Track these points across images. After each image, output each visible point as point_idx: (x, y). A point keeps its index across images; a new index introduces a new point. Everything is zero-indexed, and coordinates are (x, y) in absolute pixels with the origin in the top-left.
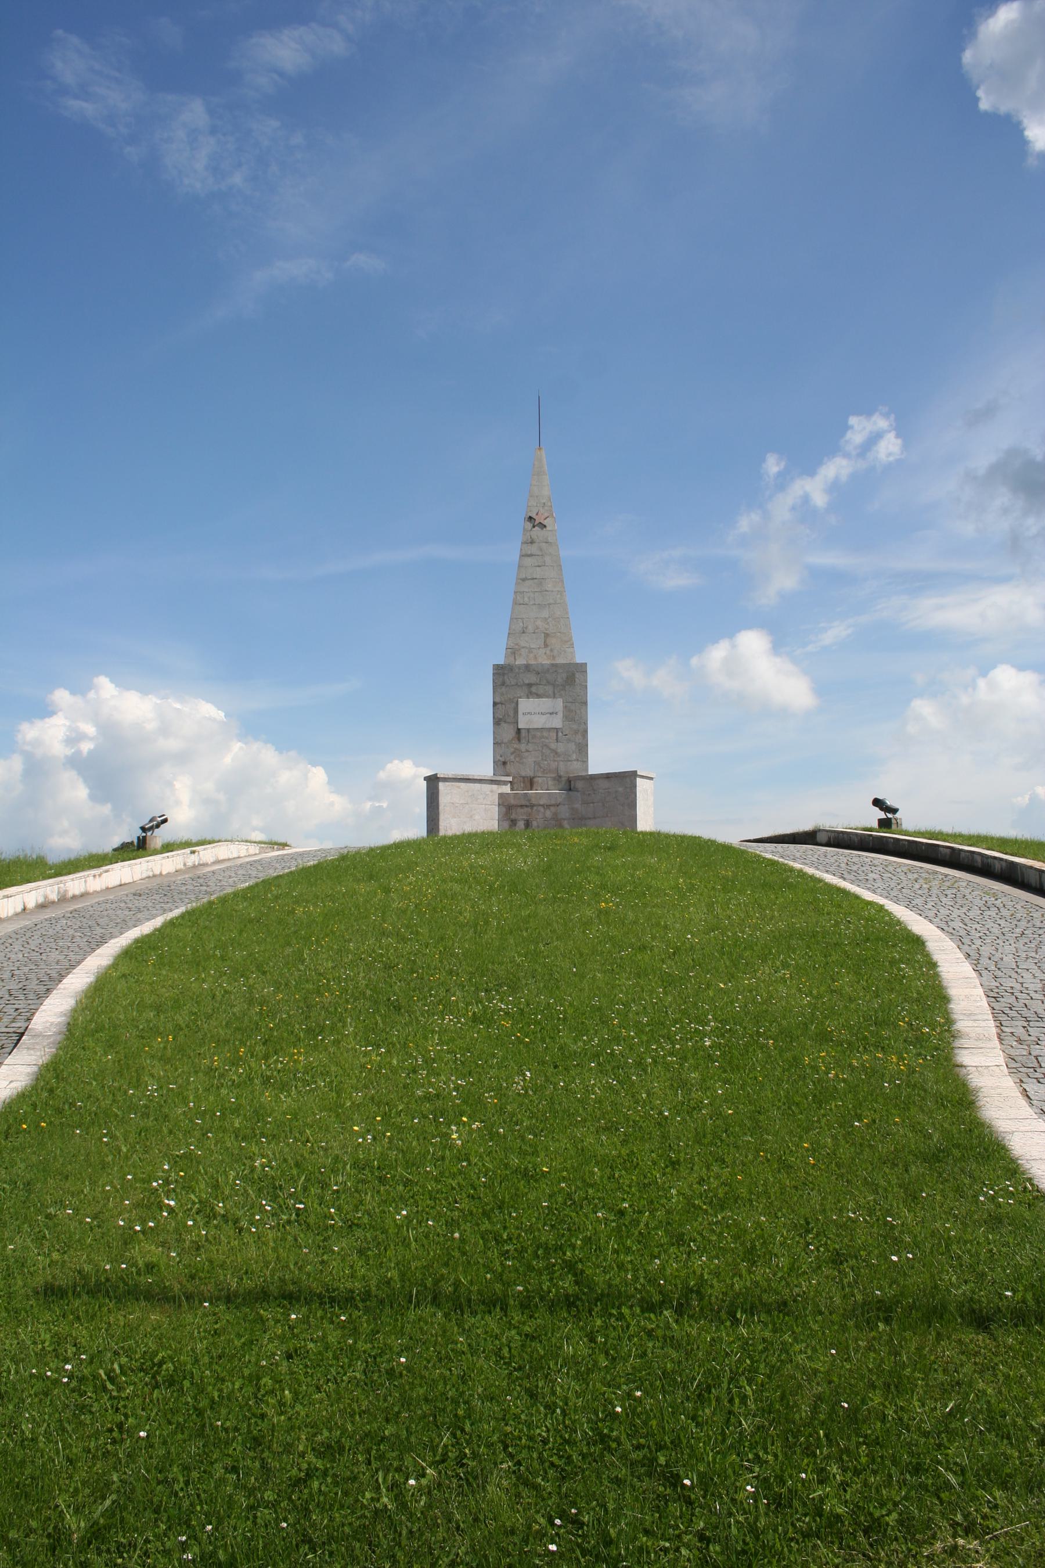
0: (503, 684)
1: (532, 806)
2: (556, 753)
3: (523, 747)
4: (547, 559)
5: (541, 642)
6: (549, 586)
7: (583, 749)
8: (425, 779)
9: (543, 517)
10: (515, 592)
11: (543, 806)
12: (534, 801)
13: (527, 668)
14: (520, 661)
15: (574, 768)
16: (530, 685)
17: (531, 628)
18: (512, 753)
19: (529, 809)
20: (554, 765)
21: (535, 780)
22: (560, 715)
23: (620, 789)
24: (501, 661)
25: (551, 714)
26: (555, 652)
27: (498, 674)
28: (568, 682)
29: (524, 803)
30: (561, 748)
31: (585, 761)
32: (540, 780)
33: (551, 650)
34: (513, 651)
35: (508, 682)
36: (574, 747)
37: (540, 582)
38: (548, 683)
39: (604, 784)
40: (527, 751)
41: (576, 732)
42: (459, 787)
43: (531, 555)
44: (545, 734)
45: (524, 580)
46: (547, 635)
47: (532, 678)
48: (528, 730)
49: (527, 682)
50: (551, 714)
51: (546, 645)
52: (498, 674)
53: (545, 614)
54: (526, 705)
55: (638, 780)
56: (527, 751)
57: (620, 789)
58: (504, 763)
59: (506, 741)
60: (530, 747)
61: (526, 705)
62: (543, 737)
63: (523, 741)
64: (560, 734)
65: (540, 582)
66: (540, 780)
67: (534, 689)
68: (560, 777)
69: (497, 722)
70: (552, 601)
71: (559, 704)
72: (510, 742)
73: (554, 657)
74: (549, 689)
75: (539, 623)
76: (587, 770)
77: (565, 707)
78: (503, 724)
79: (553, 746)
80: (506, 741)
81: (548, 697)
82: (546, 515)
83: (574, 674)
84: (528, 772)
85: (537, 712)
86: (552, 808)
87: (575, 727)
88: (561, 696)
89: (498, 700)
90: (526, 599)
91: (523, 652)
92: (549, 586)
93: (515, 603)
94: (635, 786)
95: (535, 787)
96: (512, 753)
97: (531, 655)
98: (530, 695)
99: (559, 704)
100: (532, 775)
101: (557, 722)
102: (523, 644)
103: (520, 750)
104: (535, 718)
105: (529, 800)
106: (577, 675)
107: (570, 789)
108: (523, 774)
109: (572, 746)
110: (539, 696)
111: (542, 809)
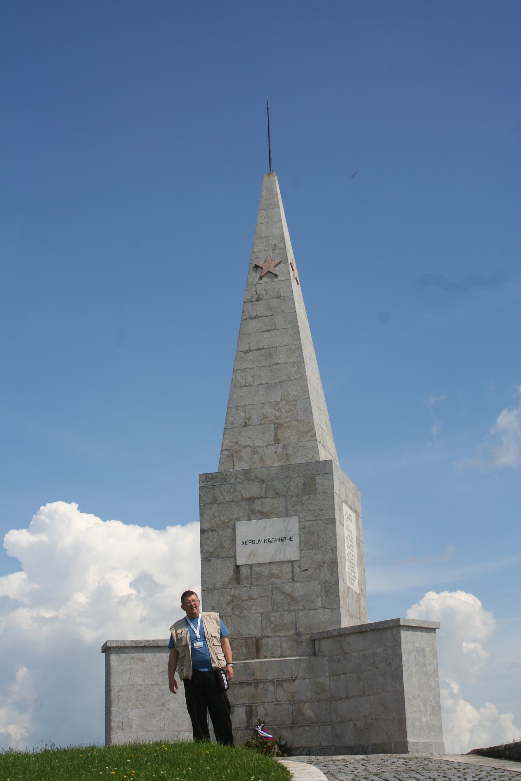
0: (214, 501)
1: (257, 683)
2: (293, 599)
3: (244, 592)
4: (279, 320)
5: (269, 437)
6: (282, 358)
7: (331, 589)
9: (273, 264)
10: (235, 371)
11: (272, 681)
12: (259, 676)
13: (248, 475)
14: (241, 466)
15: (321, 618)
16: (251, 500)
17: (255, 419)
18: (228, 604)
19: (252, 689)
20: (289, 618)
21: (264, 641)
22: (296, 540)
23: (380, 650)
24: (213, 468)
25: (283, 540)
26: (290, 450)
27: (208, 487)
28: (304, 490)
29: (244, 679)
30: (299, 590)
32: (269, 642)
33: (284, 447)
34: (230, 454)
35: (221, 499)
36: (318, 588)
37: (269, 352)
38: (278, 494)
39: (356, 643)
40: (251, 598)
41: (320, 566)
42: (143, 660)
43: (257, 317)
44: (275, 570)
45: (246, 352)
46: (278, 426)
47: (254, 489)
48: (251, 566)
49: (247, 496)
50: (283, 540)
51: (277, 441)
52: (208, 487)
53: (276, 396)
54: (245, 530)
55: (404, 635)
56: (251, 598)
57: (380, 650)
59: (219, 585)
60: (255, 592)
61: (245, 530)
62: (271, 576)
63: (245, 583)
64: (297, 569)
65: (269, 352)
66: (269, 642)
68: (299, 634)
70: (285, 378)
71: (292, 525)
72: (225, 586)
73: (288, 457)
74: (279, 503)
75: (268, 410)
76: (339, 622)
77: (302, 529)
78: (214, 561)
79: (288, 588)
80: (219, 585)
81: (278, 515)
82: (277, 260)
83: (313, 479)
84: (252, 629)
85: (263, 540)
86: (286, 685)
87: (319, 557)
88: (296, 513)
89: (207, 526)
90: (250, 378)
91: (246, 453)
92: (282, 358)
93: (234, 385)
94: (399, 645)
95: (263, 653)
96: (228, 604)
97: (256, 457)
98: (253, 514)
99: (292, 525)
100: (259, 635)
101: (291, 552)
102: (244, 441)
103: (240, 598)
104: (261, 548)
105: (253, 674)
106: (318, 479)
107: (315, 654)
108: (245, 633)
109: (316, 587)
110: (265, 515)
111: (271, 688)
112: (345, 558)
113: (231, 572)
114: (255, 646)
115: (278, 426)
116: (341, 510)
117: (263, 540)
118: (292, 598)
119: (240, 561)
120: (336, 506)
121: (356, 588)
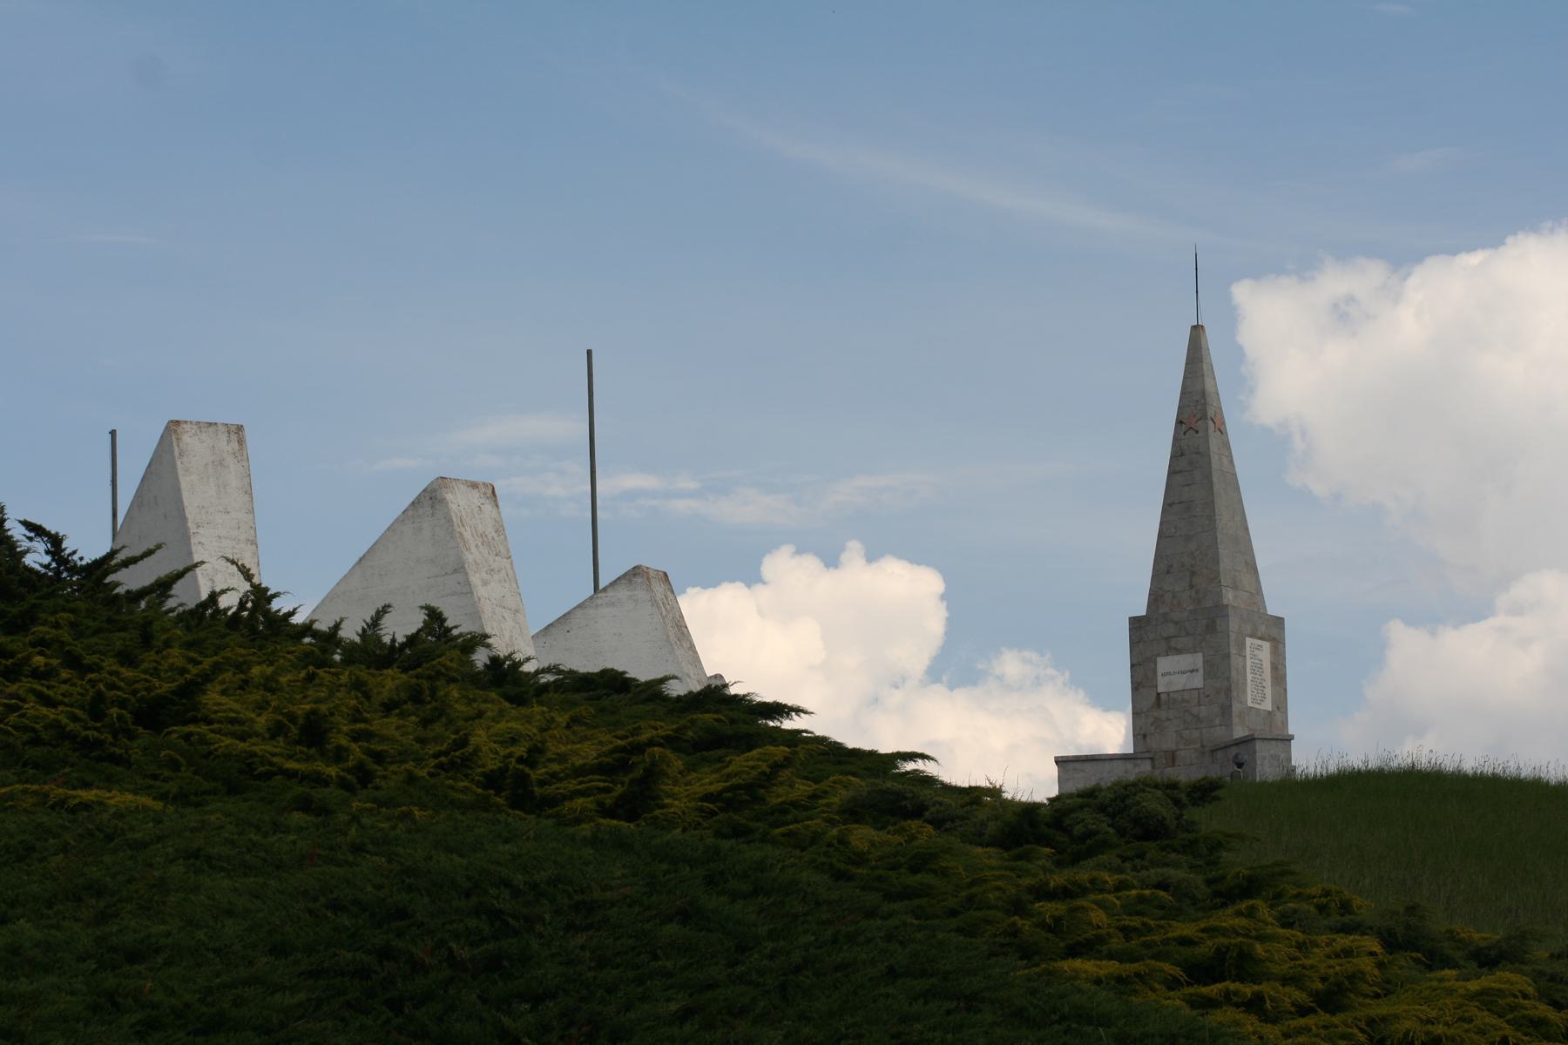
3: (1163, 714)
8: (1060, 762)
15: (1219, 734)
16: (1168, 639)
20: (1196, 734)
22: (1201, 671)
24: (1142, 611)
30: (1203, 711)
31: (1229, 725)
38: (1188, 634)
46: (1193, 573)
47: (1171, 630)
51: (1192, 587)
54: (1164, 664)
58: (1145, 736)
61: (1164, 664)
62: (1183, 701)
67: (1173, 644)
69: (1136, 687)
71: (1197, 660)
79: (1195, 710)
85: (1178, 672)
98: (1172, 650)
99: (1197, 660)
100: (1173, 747)
101: (1197, 681)
106: (1218, 621)
110: (1179, 652)
112: (1245, 684)
113: (1153, 699)
114: (1172, 757)
115: (1193, 573)
116: (1242, 646)
117: (1178, 672)
118: (1197, 718)
119: (1160, 690)
120: (1232, 643)
121: (1267, 705)
